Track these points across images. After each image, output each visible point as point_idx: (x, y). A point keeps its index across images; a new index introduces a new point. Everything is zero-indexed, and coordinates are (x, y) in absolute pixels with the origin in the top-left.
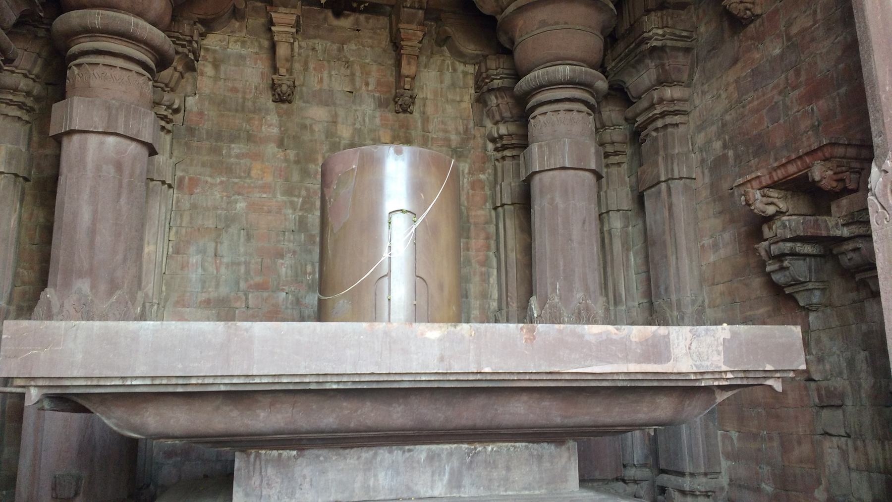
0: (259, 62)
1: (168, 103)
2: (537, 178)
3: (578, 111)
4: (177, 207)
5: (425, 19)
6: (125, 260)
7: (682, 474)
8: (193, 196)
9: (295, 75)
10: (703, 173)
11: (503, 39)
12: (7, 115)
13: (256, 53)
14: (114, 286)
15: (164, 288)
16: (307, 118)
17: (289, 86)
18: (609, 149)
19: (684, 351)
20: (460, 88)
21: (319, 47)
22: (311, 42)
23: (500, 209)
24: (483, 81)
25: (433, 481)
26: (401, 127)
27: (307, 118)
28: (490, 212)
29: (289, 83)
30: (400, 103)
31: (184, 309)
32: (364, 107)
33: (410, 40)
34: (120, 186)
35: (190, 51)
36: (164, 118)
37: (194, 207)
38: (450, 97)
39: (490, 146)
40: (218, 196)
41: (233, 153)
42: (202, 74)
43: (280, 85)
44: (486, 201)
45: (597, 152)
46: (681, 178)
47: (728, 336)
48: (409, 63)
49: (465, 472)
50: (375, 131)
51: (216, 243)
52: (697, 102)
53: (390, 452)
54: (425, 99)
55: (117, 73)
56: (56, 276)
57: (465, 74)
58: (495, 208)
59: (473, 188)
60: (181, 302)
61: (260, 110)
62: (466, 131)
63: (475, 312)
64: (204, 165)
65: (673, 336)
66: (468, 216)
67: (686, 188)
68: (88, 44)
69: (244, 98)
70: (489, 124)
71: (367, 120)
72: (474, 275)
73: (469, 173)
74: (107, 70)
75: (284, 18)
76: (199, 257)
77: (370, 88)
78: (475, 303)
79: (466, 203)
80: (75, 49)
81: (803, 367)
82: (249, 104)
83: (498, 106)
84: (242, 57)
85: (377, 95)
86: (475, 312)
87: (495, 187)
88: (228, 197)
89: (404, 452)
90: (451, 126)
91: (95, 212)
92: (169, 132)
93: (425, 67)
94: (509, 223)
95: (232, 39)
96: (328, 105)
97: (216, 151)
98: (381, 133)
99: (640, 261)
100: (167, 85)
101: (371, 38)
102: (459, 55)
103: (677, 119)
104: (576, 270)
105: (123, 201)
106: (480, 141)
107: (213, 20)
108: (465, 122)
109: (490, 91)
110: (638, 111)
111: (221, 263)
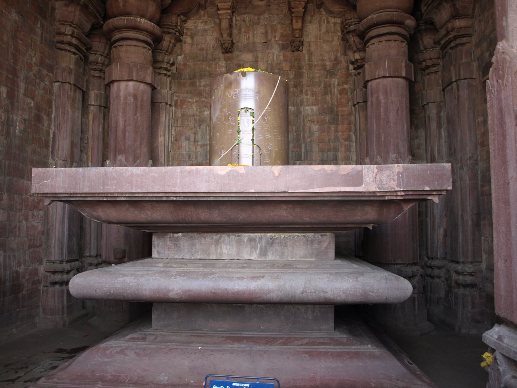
0: (214, 32)
1: (166, 61)
2: (369, 84)
3: (395, 41)
4: (175, 116)
6: (141, 144)
7: (458, 262)
8: (182, 110)
9: (234, 37)
10: (479, 74)
12: (94, 76)
13: (213, 27)
16: (241, 60)
17: (229, 44)
18: (429, 63)
19: (372, 179)
20: (332, 32)
21: (247, 19)
22: (242, 17)
23: (357, 106)
24: (344, 27)
25: (251, 252)
26: (296, 60)
27: (241, 60)
28: (351, 108)
32: (273, 50)
33: (297, 8)
34: (137, 107)
35: (176, 31)
36: (166, 69)
37: (183, 115)
38: (326, 39)
39: (351, 67)
41: (202, 85)
42: (185, 43)
43: (224, 44)
44: (348, 101)
45: (407, 66)
46: (465, 79)
47: (401, 170)
48: (297, 22)
50: (280, 64)
51: (195, 134)
52: (477, 28)
54: (310, 42)
55: (132, 49)
56: (111, 155)
57: (335, 24)
58: (354, 105)
59: (340, 94)
61: (215, 59)
62: (336, 59)
64: (187, 93)
66: (337, 111)
67: (469, 85)
68: (118, 36)
69: (207, 53)
70: (350, 53)
71: (275, 58)
72: (341, 147)
73: (338, 85)
74: (128, 48)
76: (187, 142)
79: (336, 104)
80: (113, 39)
81: (450, 188)
83: (354, 41)
84: (205, 31)
85: (281, 42)
87: (353, 92)
88: (200, 109)
89: (236, 236)
90: (326, 57)
92: (169, 76)
93: (310, 22)
94: (361, 114)
95: (200, 21)
97: (193, 84)
98: (283, 65)
99: (446, 134)
100: (167, 51)
101: (277, 9)
102: (330, 12)
103: (464, 40)
104: (392, 140)
105: (138, 114)
106: (344, 64)
107: (188, 12)
108: (335, 53)
109: (348, 32)
110: (440, 37)
111: (198, 145)
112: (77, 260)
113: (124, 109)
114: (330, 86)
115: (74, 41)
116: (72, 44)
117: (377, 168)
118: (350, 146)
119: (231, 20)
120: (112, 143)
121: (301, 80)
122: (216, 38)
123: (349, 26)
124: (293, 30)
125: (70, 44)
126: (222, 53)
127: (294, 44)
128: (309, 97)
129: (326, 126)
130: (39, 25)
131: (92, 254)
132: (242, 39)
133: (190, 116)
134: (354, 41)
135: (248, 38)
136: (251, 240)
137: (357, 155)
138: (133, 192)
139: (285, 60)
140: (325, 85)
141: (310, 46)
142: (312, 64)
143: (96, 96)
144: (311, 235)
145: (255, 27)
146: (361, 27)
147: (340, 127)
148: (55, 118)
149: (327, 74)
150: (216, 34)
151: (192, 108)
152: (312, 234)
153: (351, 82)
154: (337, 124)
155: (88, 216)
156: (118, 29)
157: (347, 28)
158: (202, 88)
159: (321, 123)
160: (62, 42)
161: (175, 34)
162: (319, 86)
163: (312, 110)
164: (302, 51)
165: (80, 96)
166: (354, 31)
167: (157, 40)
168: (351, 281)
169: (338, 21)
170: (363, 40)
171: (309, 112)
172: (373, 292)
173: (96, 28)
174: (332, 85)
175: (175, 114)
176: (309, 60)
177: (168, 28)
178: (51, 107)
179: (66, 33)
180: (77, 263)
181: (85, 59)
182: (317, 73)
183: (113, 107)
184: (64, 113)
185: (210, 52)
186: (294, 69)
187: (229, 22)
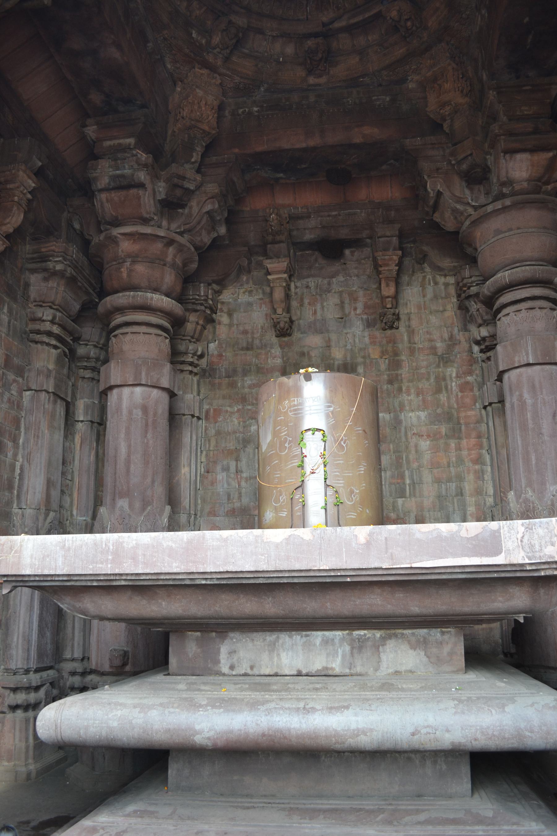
0: (263, 306)
1: (192, 352)
2: (506, 376)
5: (400, 243)
6: (153, 482)
9: (293, 312)
11: (469, 250)
12: (84, 378)
14: (146, 503)
15: (199, 501)
16: (304, 346)
17: (286, 322)
20: (442, 298)
21: (312, 285)
22: (304, 282)
23: (489, 408)
26: (388, 342)
27: (304, 346)
28: (480, 411)
29: (286, 320)
30: (384, 321)
31: (215, 518)
33: (387, 265)
35: (206, 307)
36: (191, 364)
37: (218, 433)
38: (434, 308)
39: (476, 349)
40: (236, 422)
41: (246, 385)
42: (220, 323)
48: (388, 285)
49: (356, 655)
50: (365, 349)
51: (237, 461)
53: (291, 637)
54: (409, 314)
55: (141, 337)
56: (108, 499)
57: (446, 285)
58: (485, 407)
60: (213, 513)
61: (266, 346)
62: (451, 337)
63: (471, 509)
64: (224, 397)
65: (504, 532)
66: (458, 418)
68: (119, 319)
69: (253, 338)
70: (473, 329)
71: (357, 340)
72: (468, 473)
73: (457, 377)
74: (134, 336)
75: (277, 266)
76: (224, 474)
77: (358, 312)
78: (470, 500)
80: (113, 324)
82: (257, 342)
83: (478, 310)
84: (250, 304)
85: (365, 317)
86: (471, 509)
88: (244, 422)
89: (302, 637)
90: (436, 335)
91: (129, 446)
92: (196, 374)
95: (242, 291)
96: (322, 333)
97: (232, 385)
98: (370, 351)
101: (356, 268)
102: (438, 269)
104: (549, 463)
105: (149, 435)
106: (465, 345)
108: (450, 329)
109: (469, 297)
111: (241, 478)
112: (51, 668)
113: (128, 429)
114: (444, 379)
115: (56, 329)
116: (53, 333)
117: (523, 525)
118: (483, 472)
119: (288, 288)
120: (108, 480)
121: (399, 372)
122: (266, 315)
123: (469, 288)
124: (383, 298)
125: (49, 334)
126: (276, 336)
127: (386, 318)
128: (412, 397)
129: (442, 441)
130: (5, 310)
131: (76, 656)
132: (306, 315)
133: (229, 433)
134: (478, 310)
135: (315, 313)
136: (326, 642)
137: (494, 486)
138: (140, 572)
139: (373, 343)
140: (437, 378)
141: (409, 319)
142: (415, 348)
143: (87, 407)
144: (423, 632)
145: (324, 296)
146: (487, 289)
147: (464, 442)
148: (23, 444)
149: (439, 362)
150: (265, 309)
151: (232, 421)
152: (425, 631)
153: (477, 372)
154: (460, 438)
155: (68, 608)
156: (121, 310)
157: (465, 291)
158: (246, 390)
159: (434, 437)
160: (38, 332)
161: (205, 311)
162: (428, 379)
163: (419, 418)
164: (397, 328)
165: (62, 409)
166: (477, 295)
167: (178, 323)
168: (494, 712)
169: (451, 280)
170: (492, 309)
171: (415, 421)
172: (532, 731)
173: (87, 312)
174: (448, 378)
175: (205, 431)
176: (410, 342)
177: (194, 303)
178: (18, 428)
179: (44, 318)
180: (51, 672)
181: (72, 355)
182: (423, 360)
183: (110, 424)
184: (38, 437)
185: (257, 335)
186: (387, 356)
187: (285, 291)
